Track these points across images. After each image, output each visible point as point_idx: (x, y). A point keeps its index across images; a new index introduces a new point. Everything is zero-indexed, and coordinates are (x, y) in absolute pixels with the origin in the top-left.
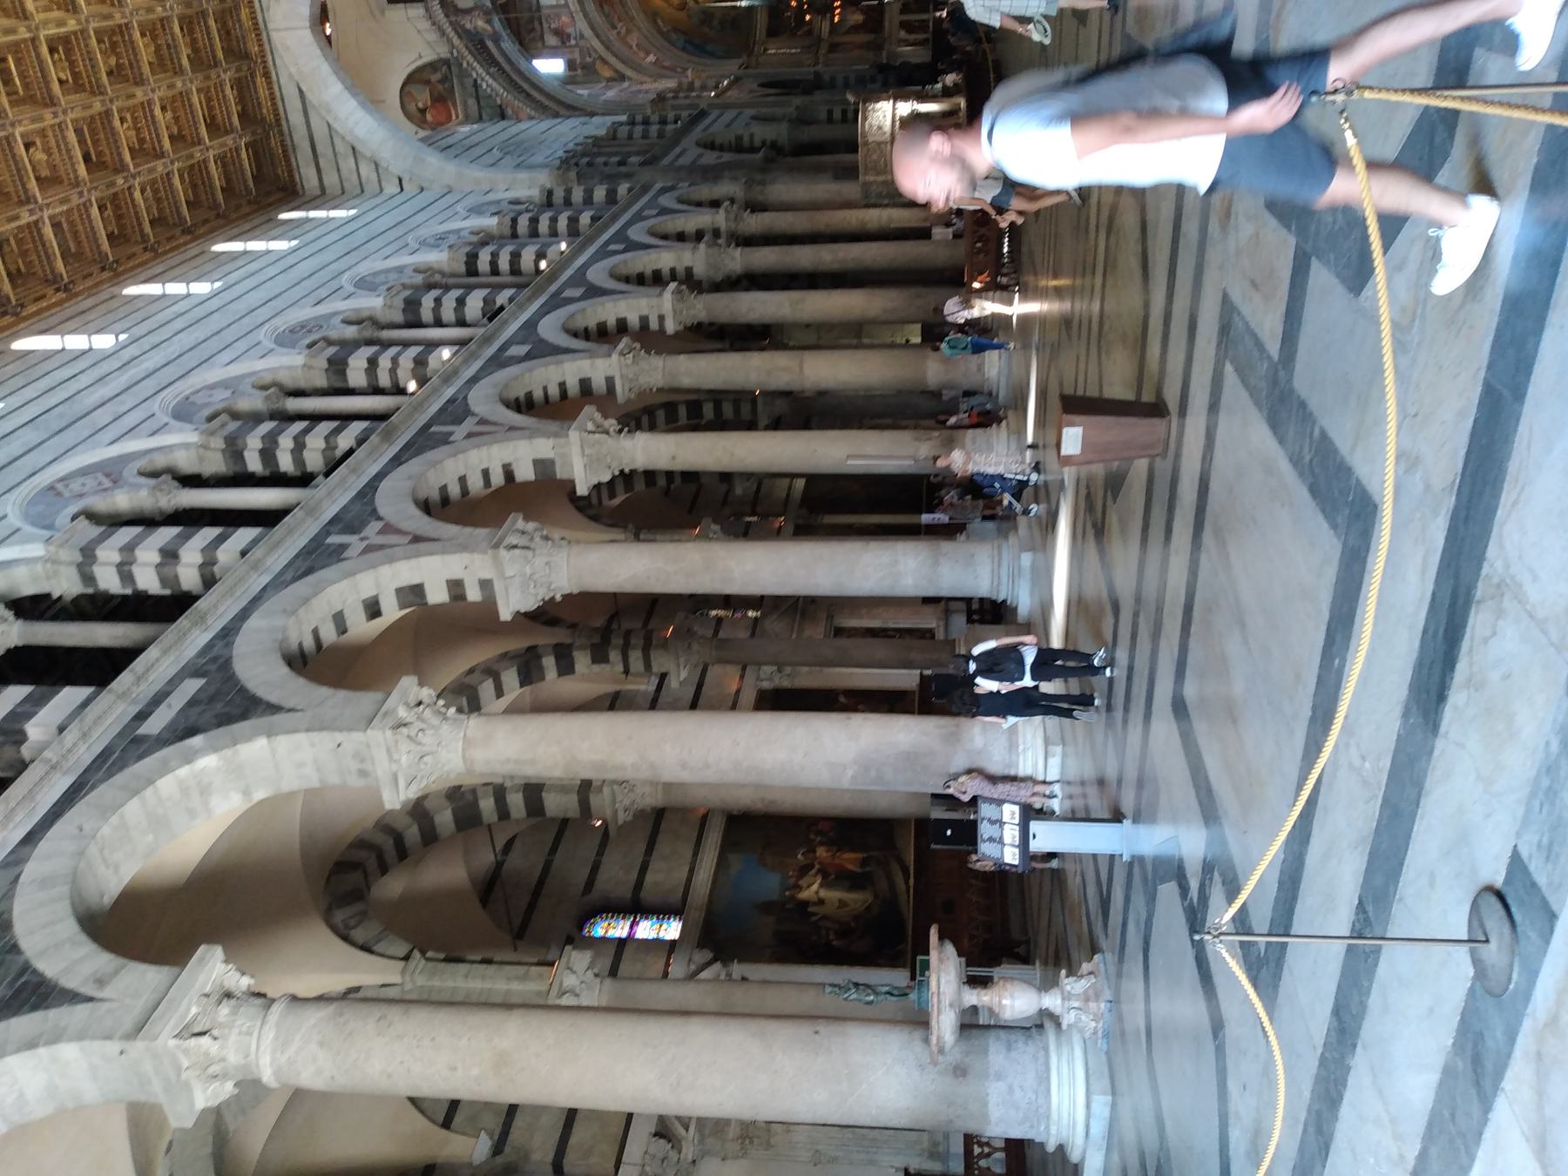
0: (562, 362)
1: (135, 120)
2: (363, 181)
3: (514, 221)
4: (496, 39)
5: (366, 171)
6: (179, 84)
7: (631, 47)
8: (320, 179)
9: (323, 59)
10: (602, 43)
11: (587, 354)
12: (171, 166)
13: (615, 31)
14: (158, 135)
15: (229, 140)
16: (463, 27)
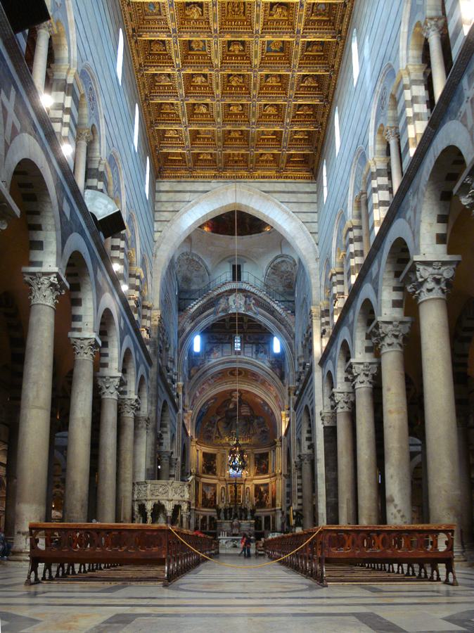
0: (56, 231)
1: (205, 87)
2: (161, 213)
3: (138, 277)
4: (215, 313)
5: (166, 216)
6: (219, 120)
7: (203, 384)
8: (163, 192)
9: (221, 205)
10: (206, 371)
11: (60, 252)
12: (179, 103)
13: (210, 378)
14: (197, 97)
15: (188, 143)
16: (221, 297)
